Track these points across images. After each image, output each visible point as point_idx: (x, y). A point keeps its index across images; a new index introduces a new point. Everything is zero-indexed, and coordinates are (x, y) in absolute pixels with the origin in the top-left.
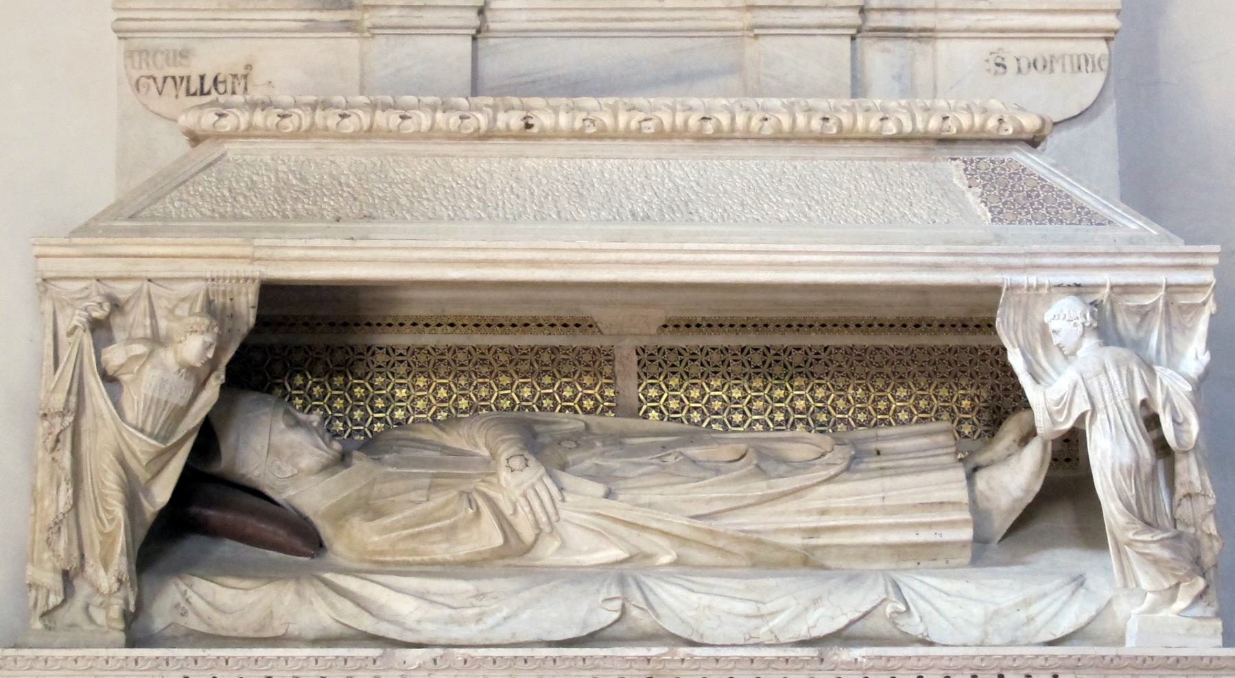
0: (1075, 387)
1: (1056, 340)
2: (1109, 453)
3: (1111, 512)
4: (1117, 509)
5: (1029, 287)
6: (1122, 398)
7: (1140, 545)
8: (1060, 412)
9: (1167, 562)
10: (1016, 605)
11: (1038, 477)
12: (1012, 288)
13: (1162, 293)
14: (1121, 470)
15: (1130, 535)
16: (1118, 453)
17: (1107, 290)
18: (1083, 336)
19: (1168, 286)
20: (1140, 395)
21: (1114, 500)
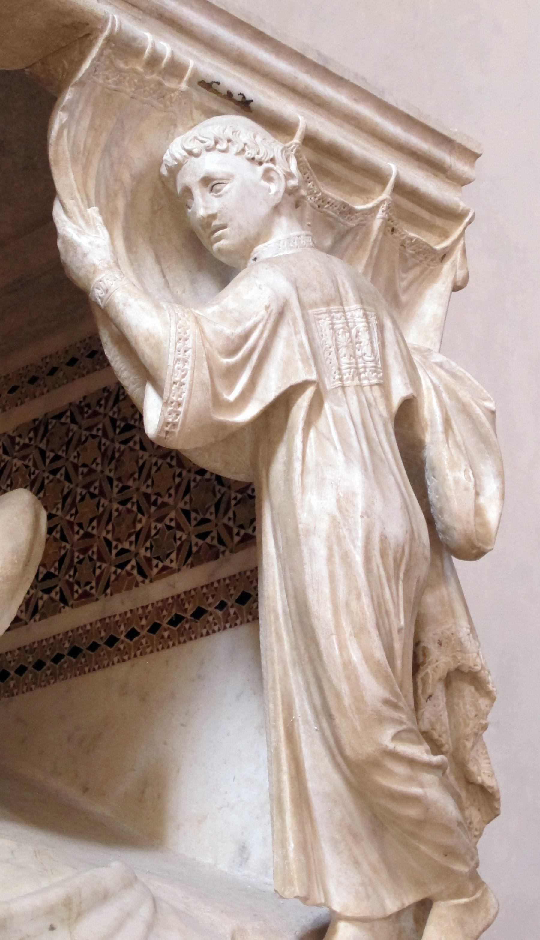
0: (281, 314)
1: (203, 205)
2: (360, 502)
3: (348, 664)
4: (368, 658)
5: (154, 60)
6: (370, 378)
7: (401, 769)
8: (231, 374)
9: (447, 829)
10: (51, 911)
11: (13, 593)
12: (124, 47)
13: (386, 194)
14: (383, 554)
15: (386, 737)
16: (378, 506)
17: (297, 139)
18: (276, 209)
19: (401, 189)
20: (400, 391)
21: (359, 632)
